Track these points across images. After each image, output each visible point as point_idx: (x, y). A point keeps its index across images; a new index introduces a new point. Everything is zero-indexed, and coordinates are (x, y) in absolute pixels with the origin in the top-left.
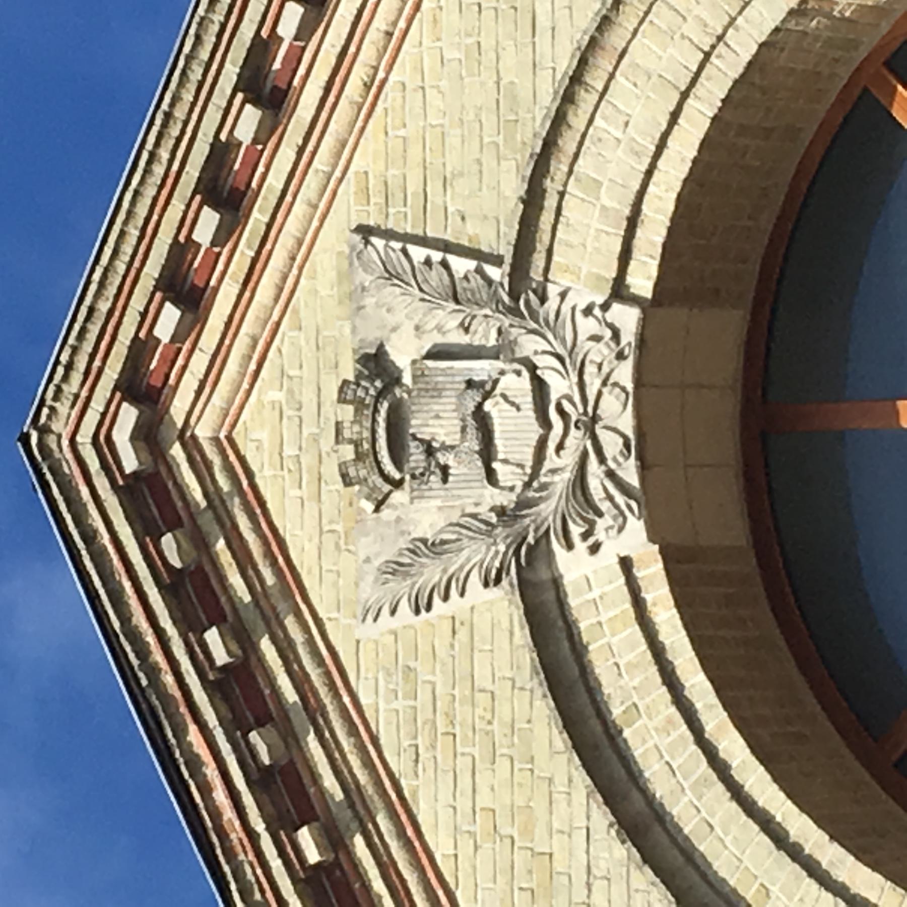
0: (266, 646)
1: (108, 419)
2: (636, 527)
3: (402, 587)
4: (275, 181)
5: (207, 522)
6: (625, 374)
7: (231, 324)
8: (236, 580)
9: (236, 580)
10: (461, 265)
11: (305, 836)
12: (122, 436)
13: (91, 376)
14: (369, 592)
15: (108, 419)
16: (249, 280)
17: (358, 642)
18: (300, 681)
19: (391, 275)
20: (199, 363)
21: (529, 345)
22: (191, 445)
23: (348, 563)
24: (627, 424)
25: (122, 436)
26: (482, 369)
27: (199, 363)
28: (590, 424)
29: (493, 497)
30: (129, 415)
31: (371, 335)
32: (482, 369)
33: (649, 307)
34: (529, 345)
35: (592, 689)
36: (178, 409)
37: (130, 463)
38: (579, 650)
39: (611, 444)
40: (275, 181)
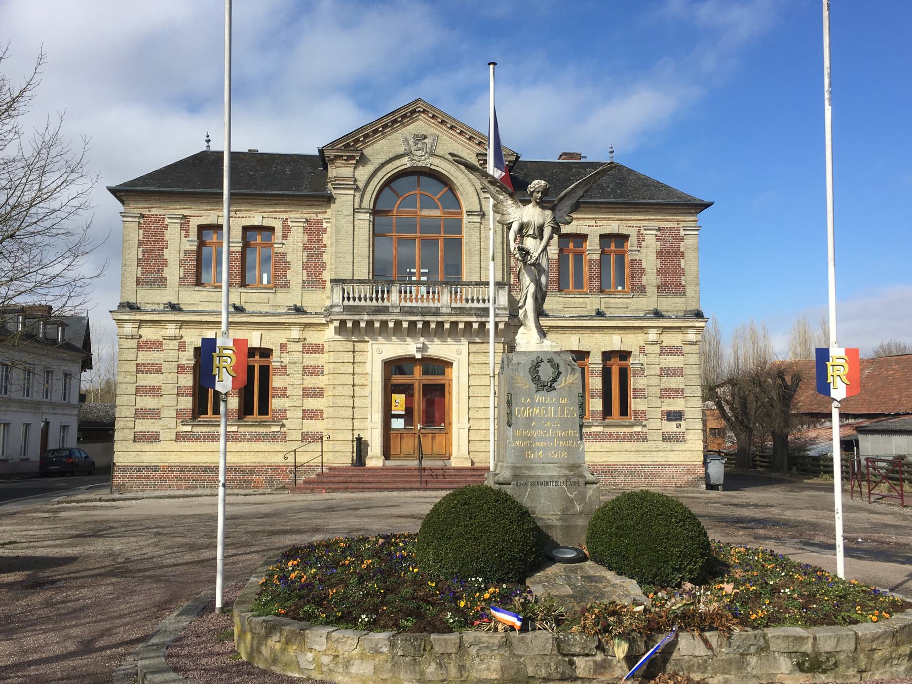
0: (399, 124)
1: (421, 108)
2: (410, 166)
3: (404, 140)
4: (443, 127)
5: (411, 117)
6: (424, 165)
7: (430, 121)
8: (405, 121)
9: (405, 121)
10: (434, 147)
11: (381, 129)
12: (420, 109)
13: (426, 107)
14: (404, 135)
15: (421, 108)
16: (434, 124)
17: (469, 222)
18: (396, 127)
19: (434, 140)
20: (426, 117)
21: (427, 155)
22: (418, 116)
23: (407, 133)
24: (419, 165)
25: (420, 109)
26: (425, 150)
27: (426, 117)
28: (419, 161)
29: (413, 151)
30: (422, 110)
31: (428, 137)
32: (425, 150)
33: (430, 167)
34: (427, 155)
35: (395, 160)
36: (422, 115)
37: (417, 110)
38: (398, 159)
39: (417, 163)
40: (443, 127)
